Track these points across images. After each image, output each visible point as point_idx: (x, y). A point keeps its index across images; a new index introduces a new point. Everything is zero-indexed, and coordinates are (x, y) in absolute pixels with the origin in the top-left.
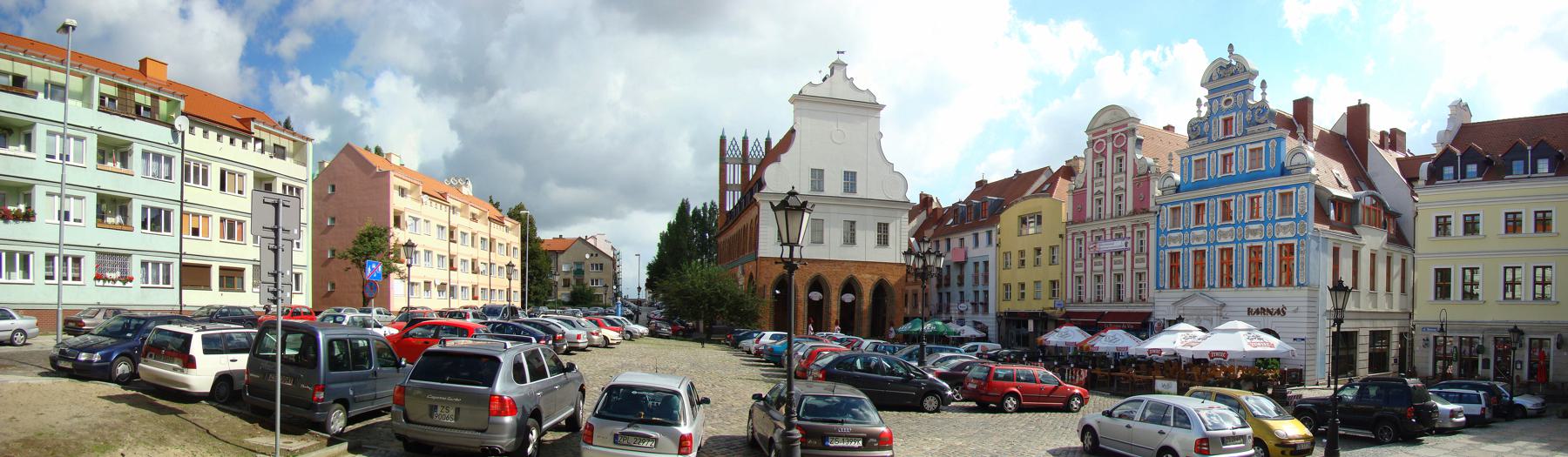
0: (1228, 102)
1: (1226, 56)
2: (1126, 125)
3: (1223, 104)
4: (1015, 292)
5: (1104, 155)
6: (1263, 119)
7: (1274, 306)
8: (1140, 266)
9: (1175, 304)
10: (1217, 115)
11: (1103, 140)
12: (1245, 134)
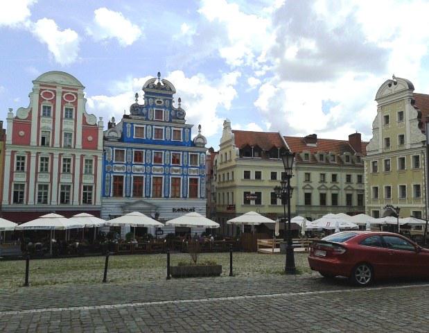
0: (158, 102)
2: (77, 90)
5: (54, 101)
6: (182, 117)
7: (189, 207)
11: (52, 93)
12: (170, 121)
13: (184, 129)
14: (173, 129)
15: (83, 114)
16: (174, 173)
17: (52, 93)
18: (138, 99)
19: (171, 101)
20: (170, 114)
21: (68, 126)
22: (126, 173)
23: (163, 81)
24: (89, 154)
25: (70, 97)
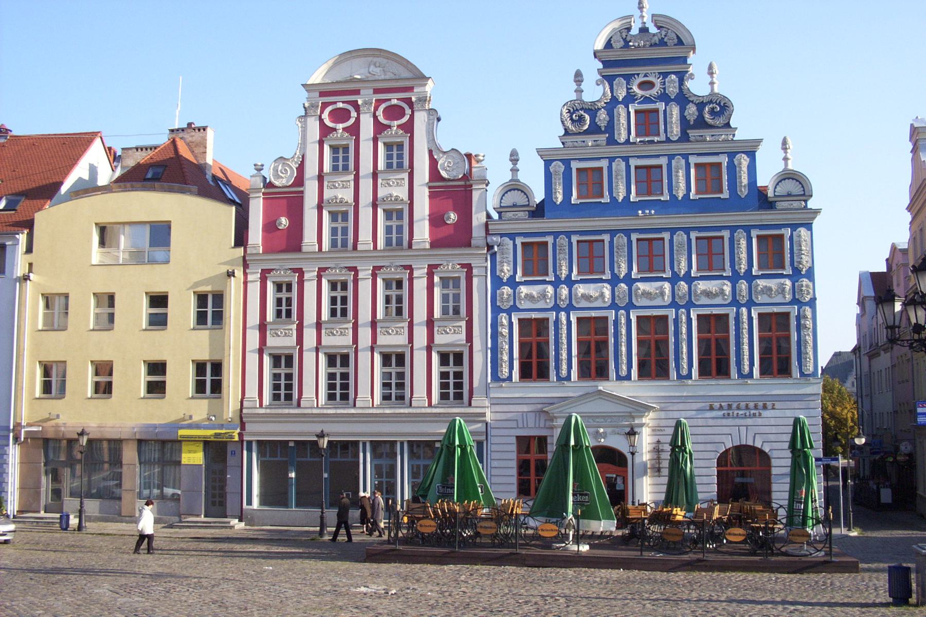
2: (410, 89)
3: (635, 88)
5: (354, 130)
6: (720, 121)
13: (732, 155)
14: (693, 160)
15: (430, 152)
18: (583, 87)
19: (682, 76)
20: (683, 118)
23: (657, 20)
25: (394, 112)
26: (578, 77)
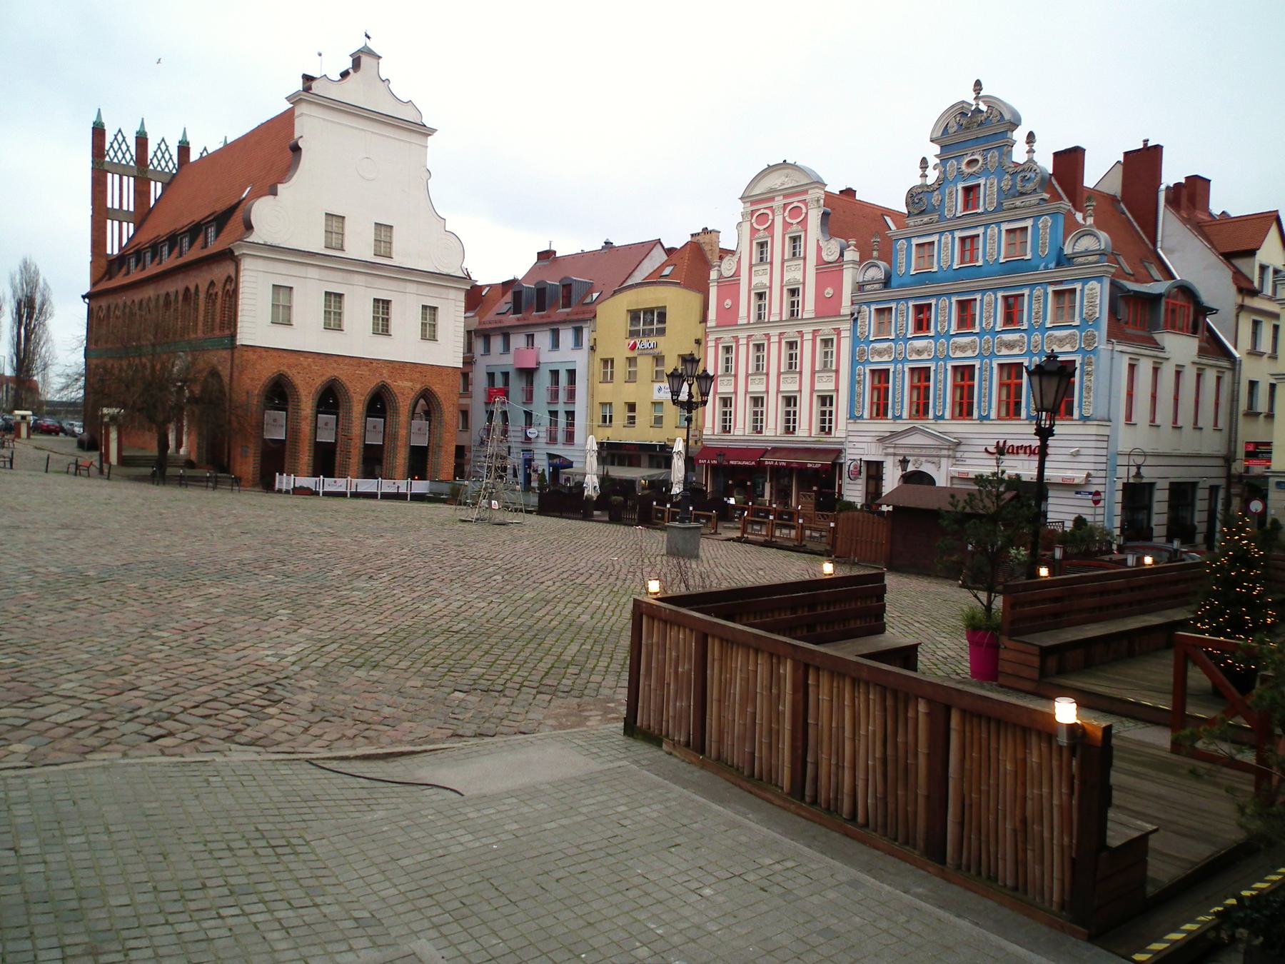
0: (970, 163)
1: (969, 97)
2: (805, 192)
3: (963, 167)
4: (620, 415)
5: (770, 229)
6: (1030, 186)
8: (825, 385)
9: (881, 440)
10: (955, 182)
11: (766, 211)
15: (818, 241)
16: (1004, 351)
17: (766, 211)
20: (1000, 189)
21: (794, 275)
22: (895, 361)
24: (826, 330)
26: (924, 161)
